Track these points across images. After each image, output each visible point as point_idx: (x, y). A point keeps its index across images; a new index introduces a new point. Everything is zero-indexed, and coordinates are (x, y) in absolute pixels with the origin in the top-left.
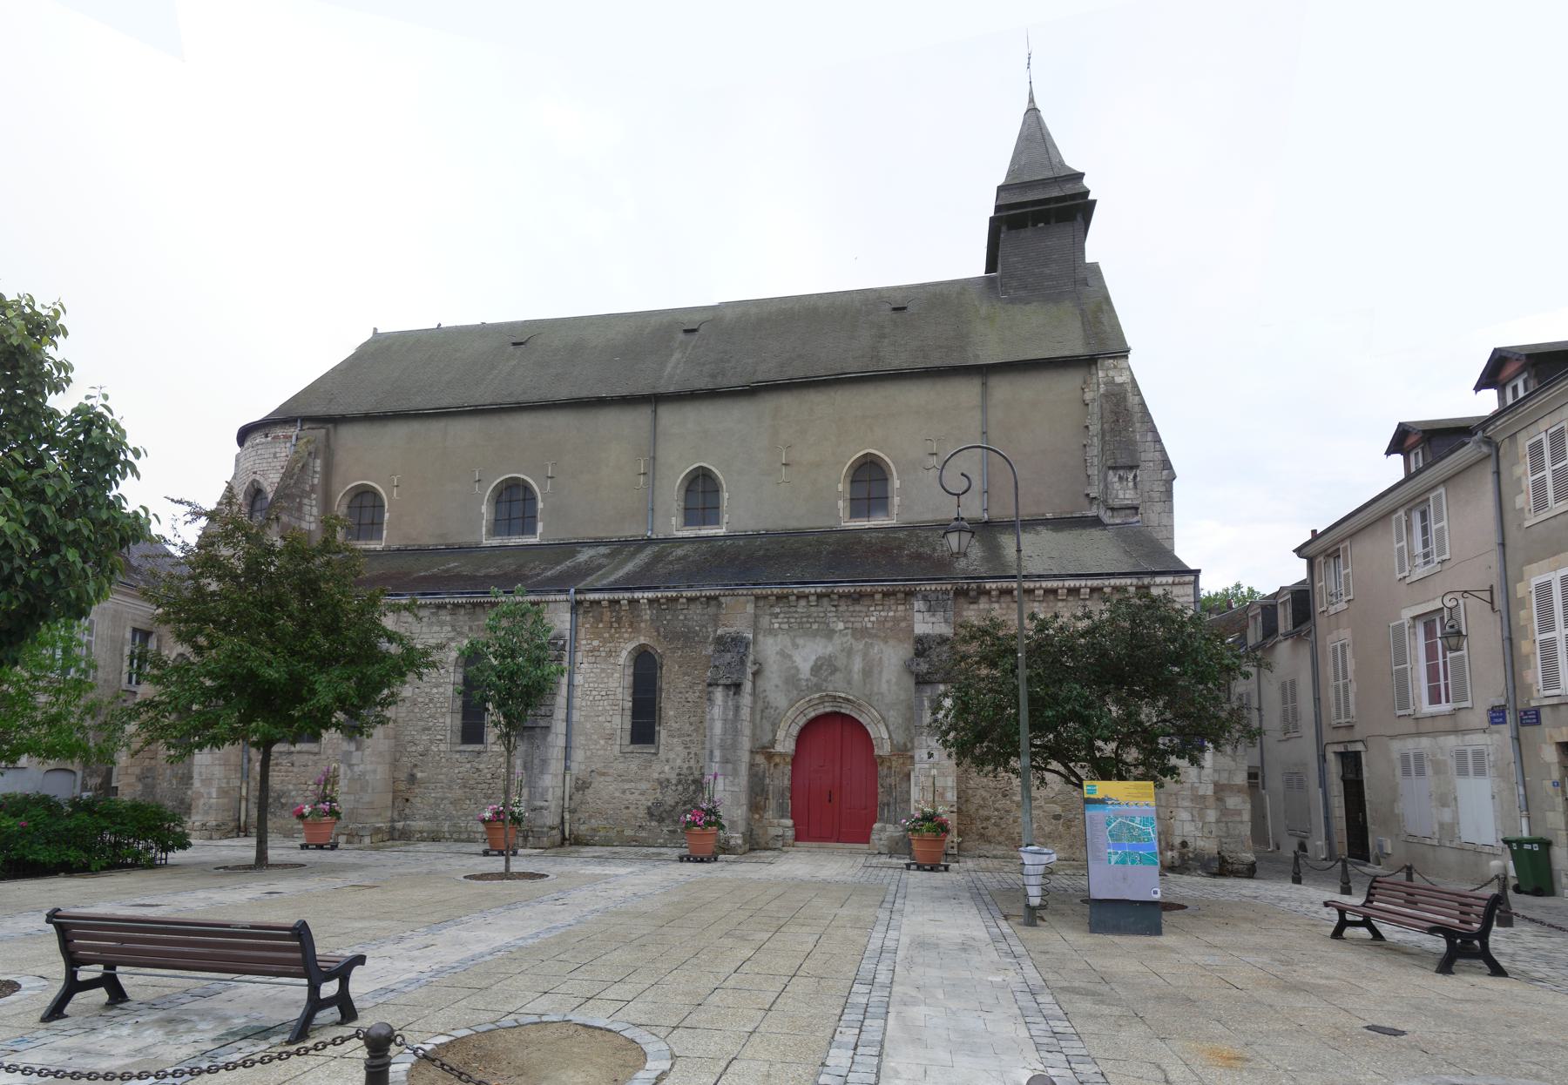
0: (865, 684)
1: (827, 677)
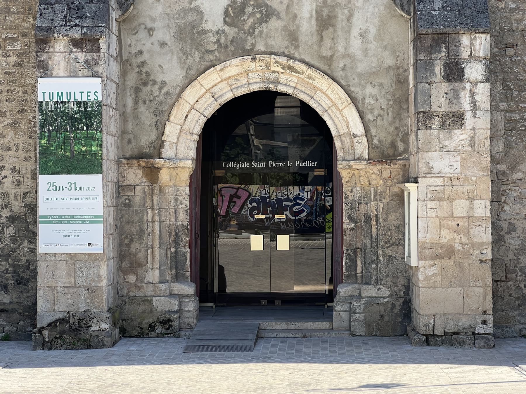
0: (322, 39)
1: (253, 27)
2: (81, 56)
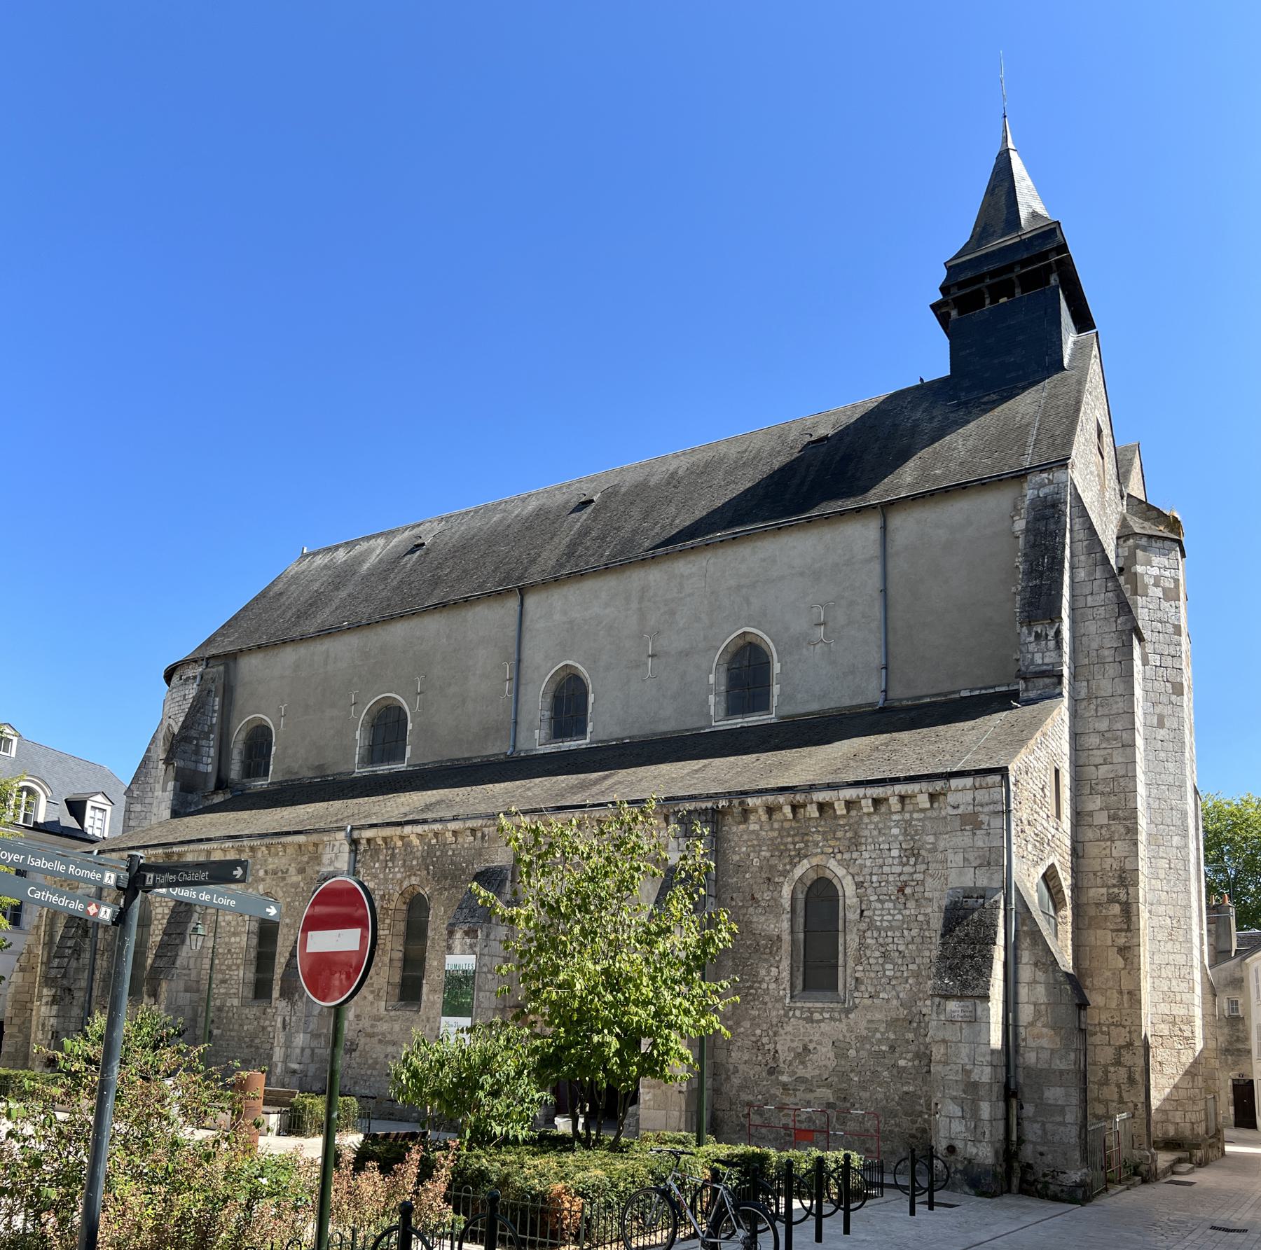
2: (468, 941)
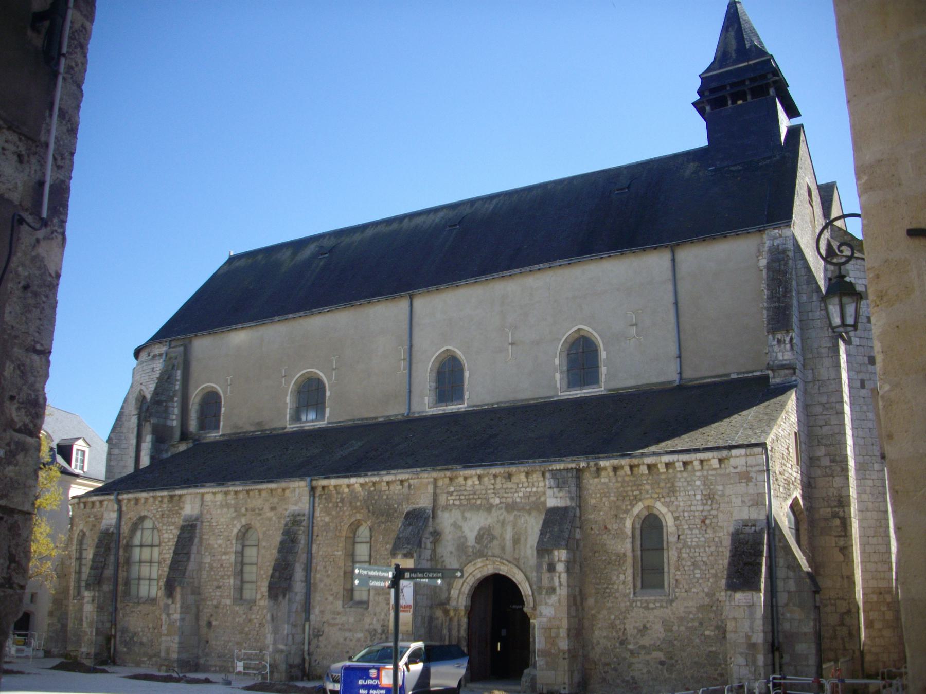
0: (514, 550)
1: (487, 544)
